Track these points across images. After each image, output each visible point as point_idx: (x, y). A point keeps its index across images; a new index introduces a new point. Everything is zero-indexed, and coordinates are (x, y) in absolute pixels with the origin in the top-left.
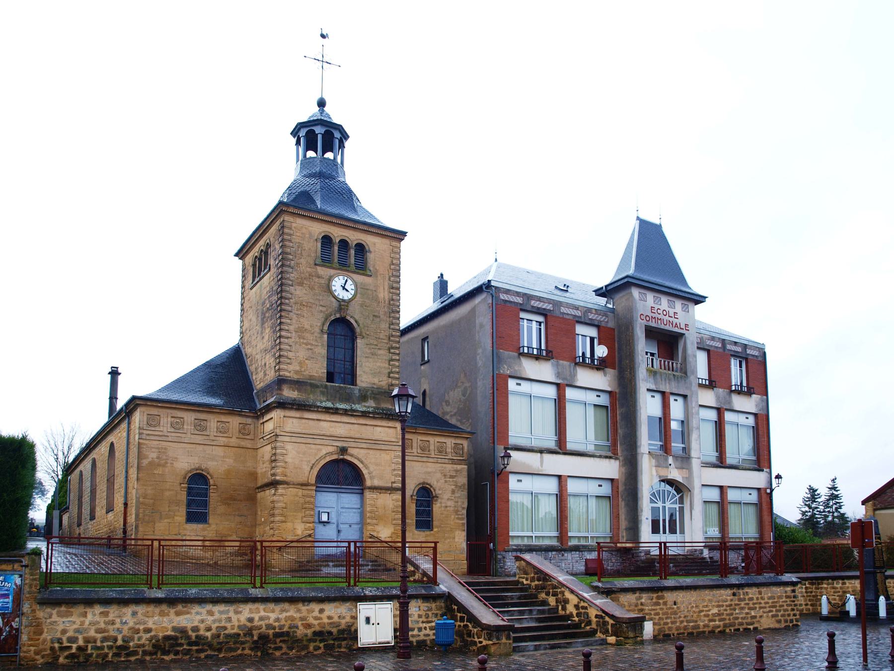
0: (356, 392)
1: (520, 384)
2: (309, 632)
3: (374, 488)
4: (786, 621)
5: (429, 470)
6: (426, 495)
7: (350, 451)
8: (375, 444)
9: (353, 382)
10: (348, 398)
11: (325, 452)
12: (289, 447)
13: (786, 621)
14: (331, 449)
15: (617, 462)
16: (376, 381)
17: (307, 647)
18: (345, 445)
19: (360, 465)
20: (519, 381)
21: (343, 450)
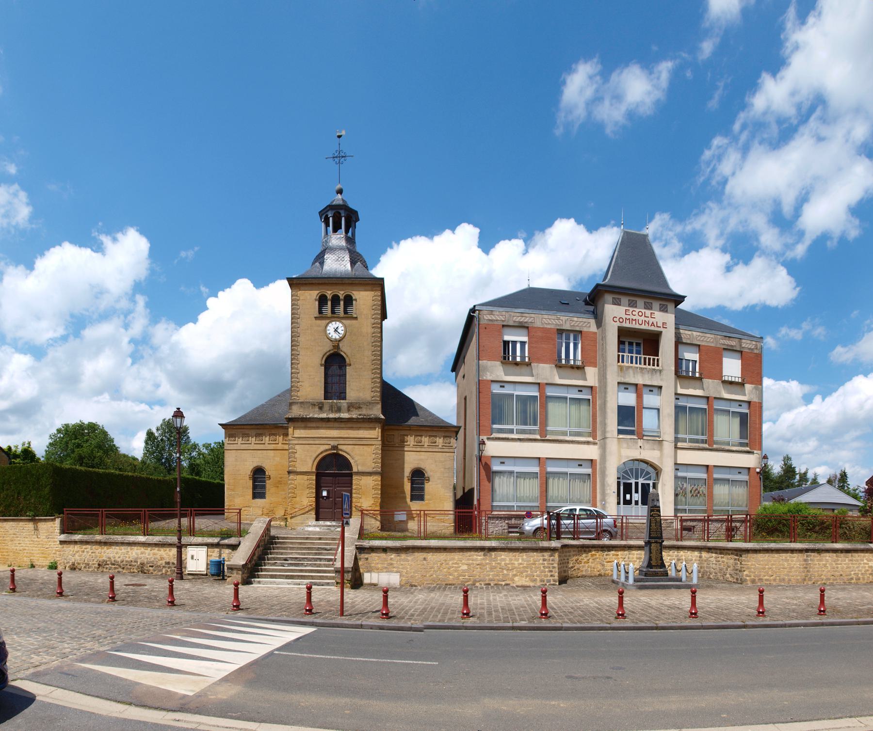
0: (345, 405)
1: (503, 387)
2: (163, 562)
3: (359, 473)
4: (542, 581)
5: (422, 457)
6: (418, 475)
7: (340, 447)
8: (360, 442)
9: (344, 398)
10: (339, 410)
11: (322, 449)
12: (297, 447)
13: (542, 581)
14: (327, 447)
15: (596, 447)
16: (361, 395)
17: (161, 570)
18: (333, 443)
19: (348, 457)
20: (502, 384)
21: (335, 447)
